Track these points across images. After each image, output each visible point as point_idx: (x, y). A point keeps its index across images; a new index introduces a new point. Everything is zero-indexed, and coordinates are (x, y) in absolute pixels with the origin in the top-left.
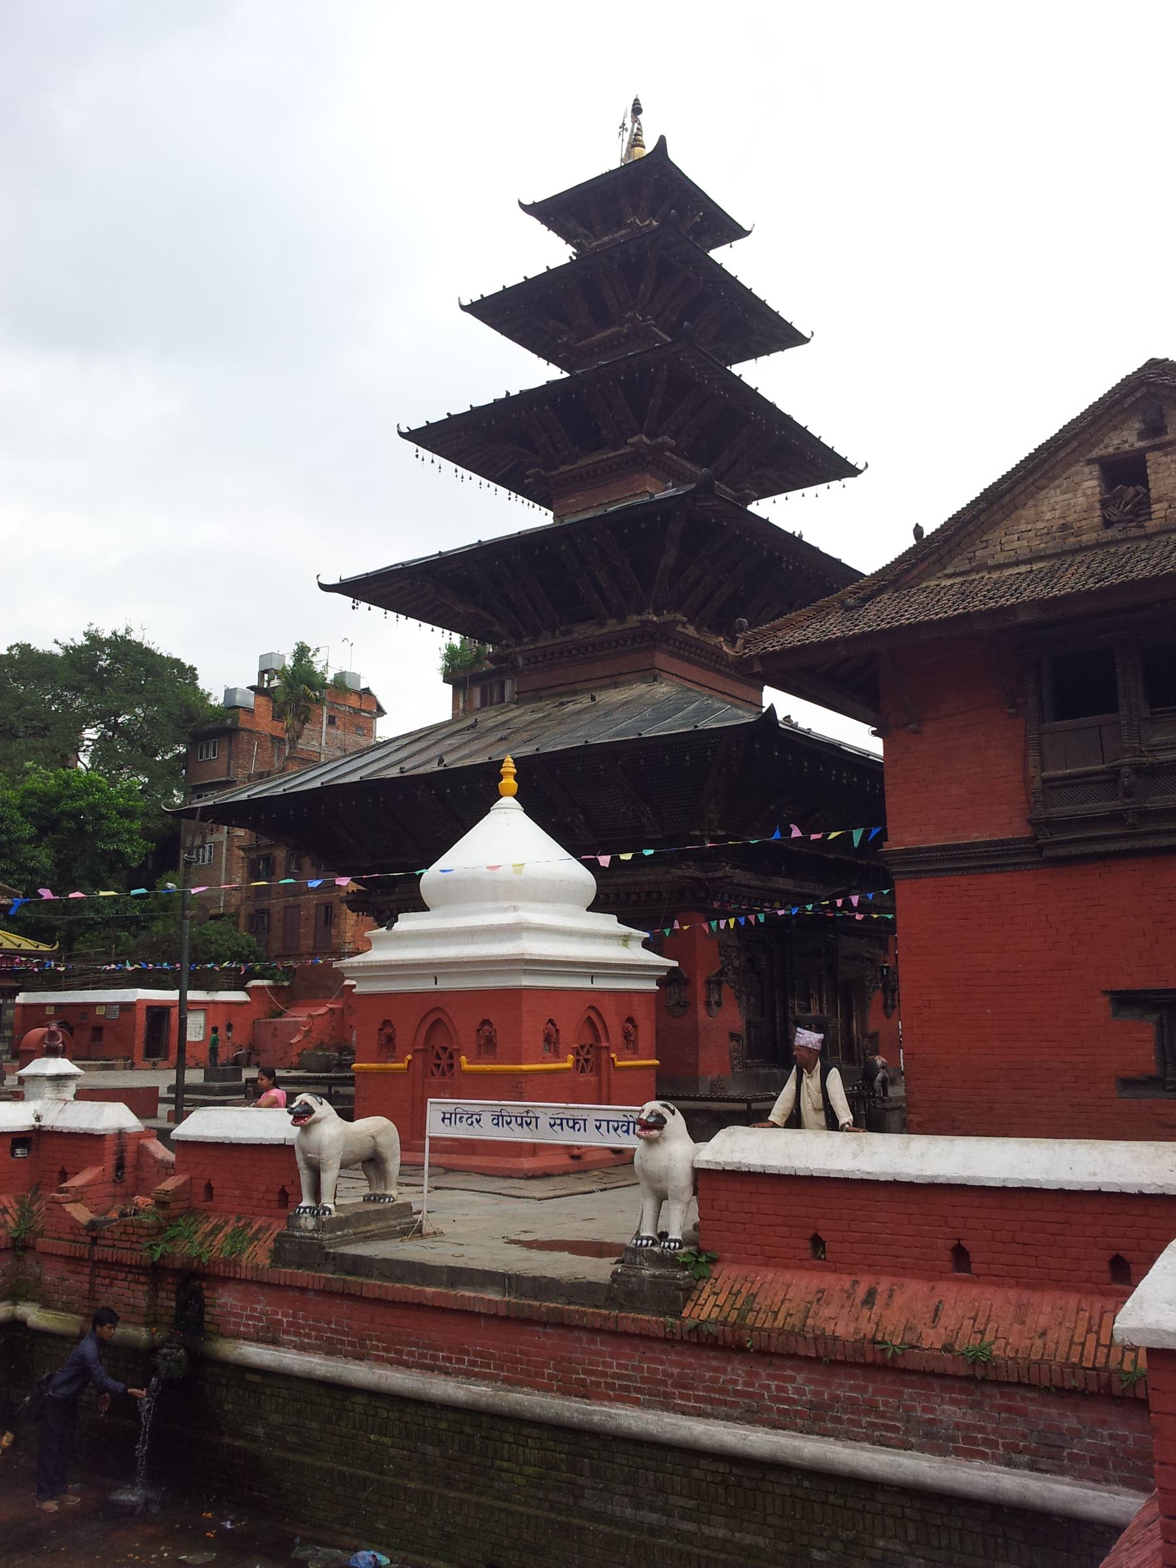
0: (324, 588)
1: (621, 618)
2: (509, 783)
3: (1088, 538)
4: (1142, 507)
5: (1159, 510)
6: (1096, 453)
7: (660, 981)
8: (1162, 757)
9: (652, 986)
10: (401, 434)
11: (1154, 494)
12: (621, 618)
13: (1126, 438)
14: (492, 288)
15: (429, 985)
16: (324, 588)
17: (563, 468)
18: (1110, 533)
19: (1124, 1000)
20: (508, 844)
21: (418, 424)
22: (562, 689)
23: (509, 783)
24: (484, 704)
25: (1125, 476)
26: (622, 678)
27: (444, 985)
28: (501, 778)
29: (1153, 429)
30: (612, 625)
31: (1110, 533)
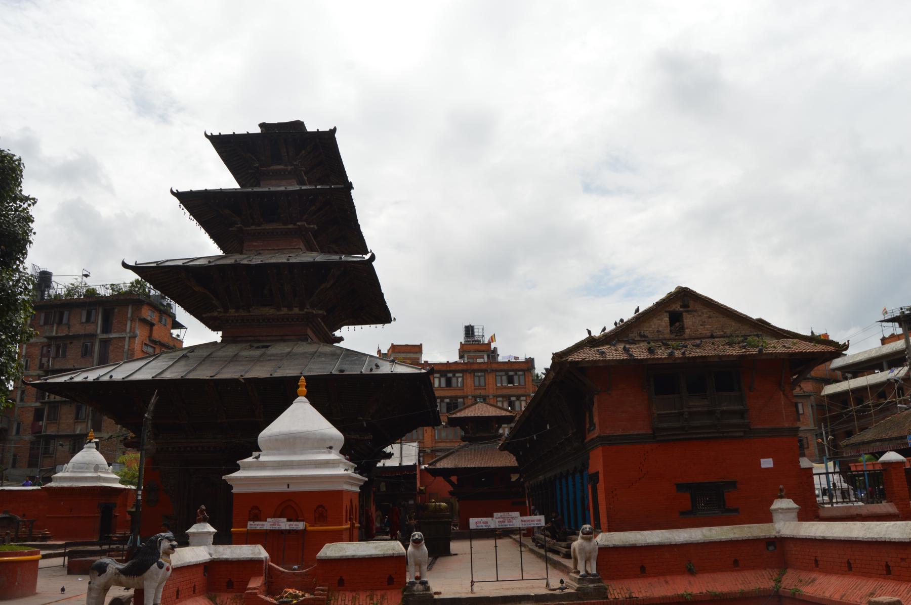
0: (125, 265)
1: (290, 308)
2: (302, 389)
3: (667, 336)
4: (682, 329)
5: (687, 331)
6: (668, 309)
7: (361, 487)
8: (695, 409)
9: (357, 489)
10: (172, 192)
11: (686, 326)
12: (290, 308)
13: (677, 307)
14: (227, 130)
15: (283, 488)
16: (125, 265)
17: (253, 227)
18: (673, 336)
19: (680, 487)
20: (301, 418)
21: (182, 189)
22: (250, 338)
23: (302, 389)
24: (45, 323)
25: (675, 318)
26: (287, 338)
27: (293, 488)
28: (298, 387)
29: (685, 306)
30: (285, 311)
31: (673, 336)
